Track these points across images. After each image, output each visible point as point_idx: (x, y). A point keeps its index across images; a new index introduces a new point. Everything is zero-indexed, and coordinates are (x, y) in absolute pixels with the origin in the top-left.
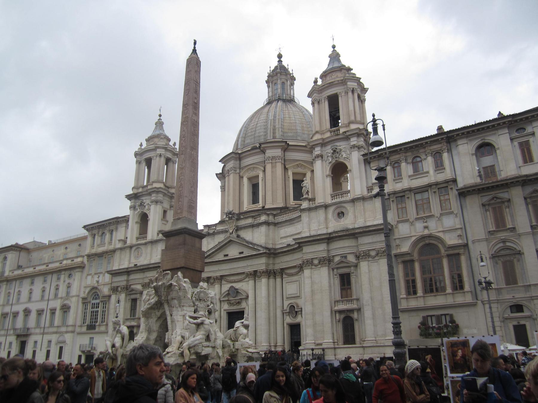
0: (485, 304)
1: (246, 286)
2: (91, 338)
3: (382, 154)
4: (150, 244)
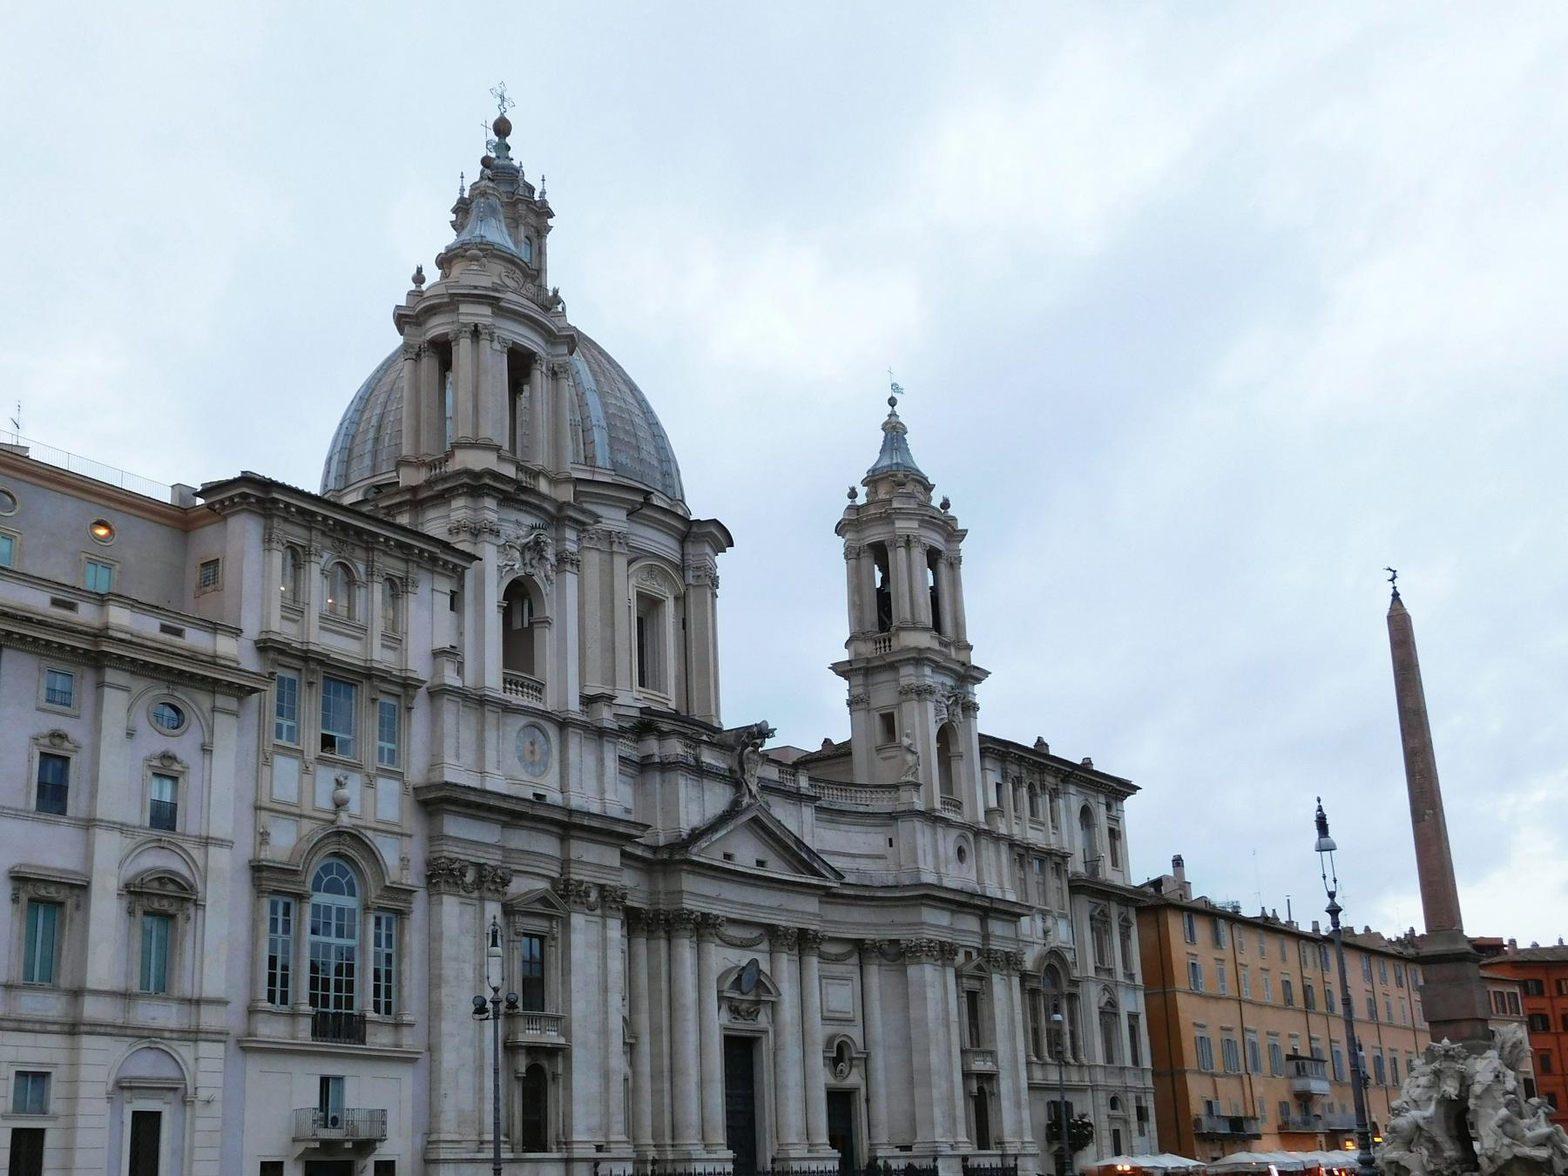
0: (1098, 1090)
1: (785, 969)
2: (325, 1081)
3: (1012, 752)
4: (582, 732)
